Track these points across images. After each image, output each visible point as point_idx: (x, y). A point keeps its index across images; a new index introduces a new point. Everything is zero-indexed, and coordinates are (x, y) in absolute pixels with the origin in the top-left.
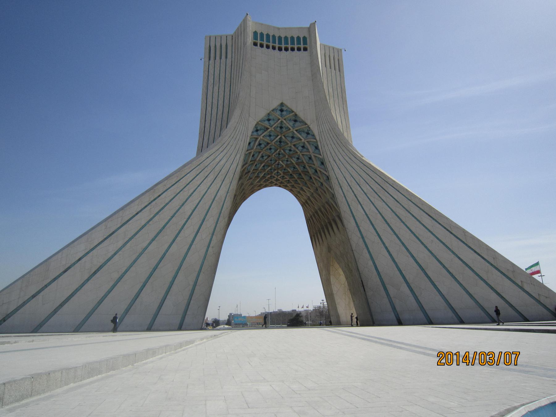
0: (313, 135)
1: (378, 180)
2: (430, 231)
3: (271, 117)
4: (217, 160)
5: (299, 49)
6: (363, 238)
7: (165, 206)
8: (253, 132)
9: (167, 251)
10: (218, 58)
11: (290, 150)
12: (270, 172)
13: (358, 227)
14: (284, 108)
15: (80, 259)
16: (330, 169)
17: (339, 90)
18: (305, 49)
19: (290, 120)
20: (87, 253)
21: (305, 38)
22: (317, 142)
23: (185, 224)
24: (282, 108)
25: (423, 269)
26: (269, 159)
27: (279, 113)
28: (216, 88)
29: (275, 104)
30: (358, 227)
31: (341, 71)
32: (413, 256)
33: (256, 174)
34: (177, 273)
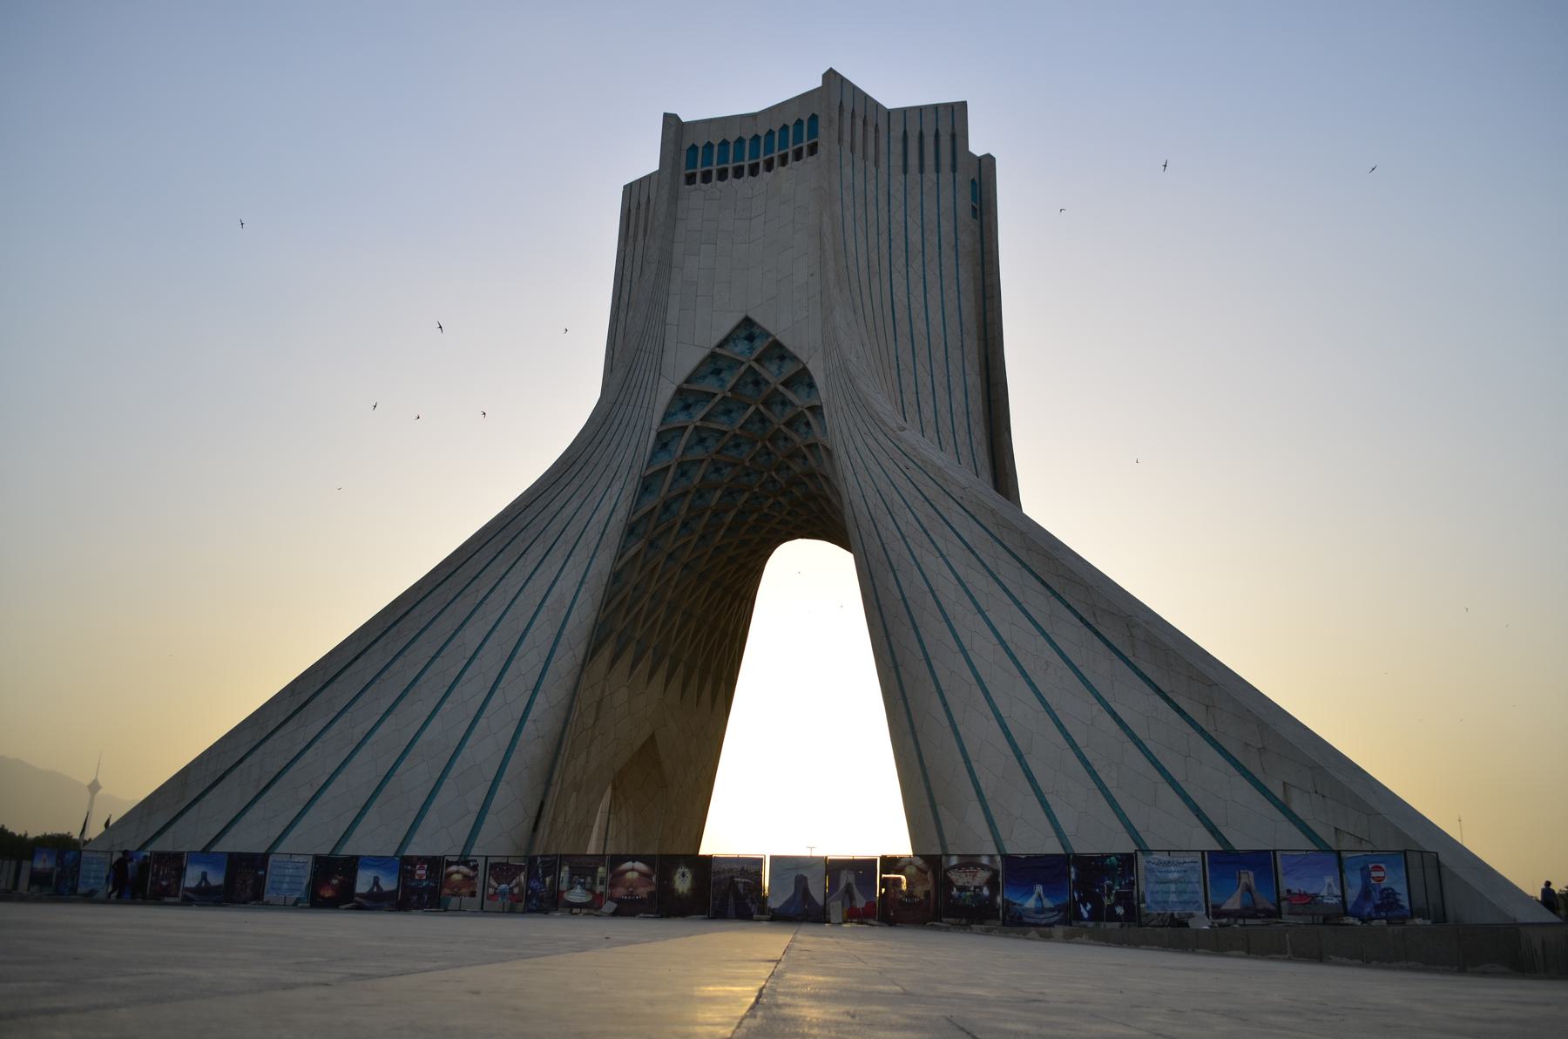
1: (931, 491)
2: (1043, 633)
7: (418, 635)
9: (418, 735)
10: (640, 237)
14: (757, 331)
21: (814, 118)
25: (1020, 757)
29: (727, 324)
32: (999, 717)
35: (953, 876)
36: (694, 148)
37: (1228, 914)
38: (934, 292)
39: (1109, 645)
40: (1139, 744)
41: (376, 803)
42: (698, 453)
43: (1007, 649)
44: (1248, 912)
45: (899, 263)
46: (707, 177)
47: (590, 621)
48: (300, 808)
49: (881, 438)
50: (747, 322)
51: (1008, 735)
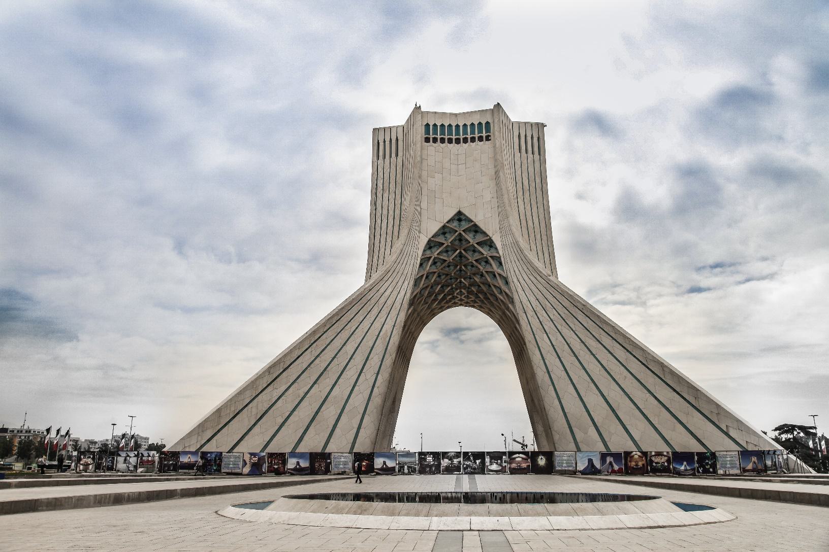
0: (496, 249)
1: (566, 303)
2: (623, 365)
3: (446, 230)
5: (481, 139)
8: (424, 251)
11: (472, 266)
12: (451, 292)
14: (462, 217)
16: (513, 289)
17: (538, 180)
18: (488, 138)
22: (500, 258)
24: (460, 217)
27: (456, 223)
29: (451, 213)
35: (653, 459)
36: (427, 125)
37: (748, 471)
38: (535, 209)
39: (653, 372)
43: (606, 370)
44: (753, 470)
45: (520, 194)
46: (435, 140)
47: (397, 343)
48: (277, 428)
50: (460, 213)
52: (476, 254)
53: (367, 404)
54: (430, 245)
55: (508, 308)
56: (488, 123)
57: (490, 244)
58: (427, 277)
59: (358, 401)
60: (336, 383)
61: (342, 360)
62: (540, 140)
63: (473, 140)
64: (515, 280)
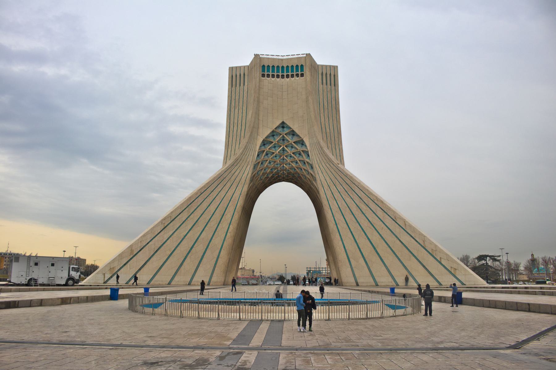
0: (306, 146)
2: (382, 221)
3: (274, 134)
4: (233, 172)
5: (297, 75)
6: (336, 224)
8: (260, 147)
9: (199, 236)
10: (238, 85)
11: (291, 157)
13: (333, 216)
14: (285, 126)
15: (148, 243)
16: (316, 172)
17: (334, 103)
18: (302, 75)
19: (289, 134)
20: (152, 239)
21: (302, 66)
22: (308, 152)
23: (210, 219)
24: (283, 125)
25: (375, 248)
26: (276, 163)
28: (237, 110)
29: (278, 123)
30: (333, 216)
31: (336, 85)
32: (369, 239)
33: (266, 176)
34: (206, 250)
40: (407, 248)
41: (189, 255)
42: (266, 158)
43: (371, 223)
45: (322, 111)
46: (268, 76)
49: (332, 165)
50: (283, 123)
51: (371, 243)
52: (293, 149)
53: (223, 243)
54: (264, 143)
55: (313, 184)
56: (302, 66)
57: (302, 143)
58: (262, 163)
59: (217, 241)
60: (203, 230)
61: (207, 216)
62: (336, 77)
63: (292, 76)
64: (317, 166)
